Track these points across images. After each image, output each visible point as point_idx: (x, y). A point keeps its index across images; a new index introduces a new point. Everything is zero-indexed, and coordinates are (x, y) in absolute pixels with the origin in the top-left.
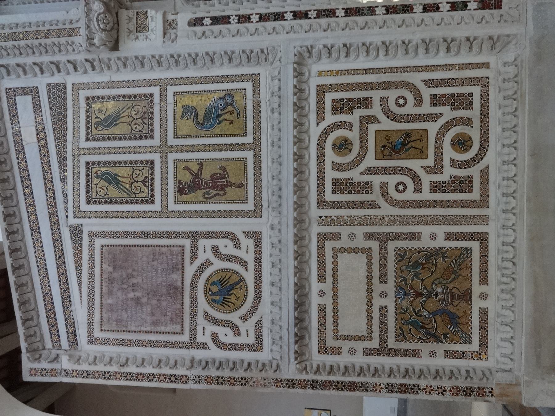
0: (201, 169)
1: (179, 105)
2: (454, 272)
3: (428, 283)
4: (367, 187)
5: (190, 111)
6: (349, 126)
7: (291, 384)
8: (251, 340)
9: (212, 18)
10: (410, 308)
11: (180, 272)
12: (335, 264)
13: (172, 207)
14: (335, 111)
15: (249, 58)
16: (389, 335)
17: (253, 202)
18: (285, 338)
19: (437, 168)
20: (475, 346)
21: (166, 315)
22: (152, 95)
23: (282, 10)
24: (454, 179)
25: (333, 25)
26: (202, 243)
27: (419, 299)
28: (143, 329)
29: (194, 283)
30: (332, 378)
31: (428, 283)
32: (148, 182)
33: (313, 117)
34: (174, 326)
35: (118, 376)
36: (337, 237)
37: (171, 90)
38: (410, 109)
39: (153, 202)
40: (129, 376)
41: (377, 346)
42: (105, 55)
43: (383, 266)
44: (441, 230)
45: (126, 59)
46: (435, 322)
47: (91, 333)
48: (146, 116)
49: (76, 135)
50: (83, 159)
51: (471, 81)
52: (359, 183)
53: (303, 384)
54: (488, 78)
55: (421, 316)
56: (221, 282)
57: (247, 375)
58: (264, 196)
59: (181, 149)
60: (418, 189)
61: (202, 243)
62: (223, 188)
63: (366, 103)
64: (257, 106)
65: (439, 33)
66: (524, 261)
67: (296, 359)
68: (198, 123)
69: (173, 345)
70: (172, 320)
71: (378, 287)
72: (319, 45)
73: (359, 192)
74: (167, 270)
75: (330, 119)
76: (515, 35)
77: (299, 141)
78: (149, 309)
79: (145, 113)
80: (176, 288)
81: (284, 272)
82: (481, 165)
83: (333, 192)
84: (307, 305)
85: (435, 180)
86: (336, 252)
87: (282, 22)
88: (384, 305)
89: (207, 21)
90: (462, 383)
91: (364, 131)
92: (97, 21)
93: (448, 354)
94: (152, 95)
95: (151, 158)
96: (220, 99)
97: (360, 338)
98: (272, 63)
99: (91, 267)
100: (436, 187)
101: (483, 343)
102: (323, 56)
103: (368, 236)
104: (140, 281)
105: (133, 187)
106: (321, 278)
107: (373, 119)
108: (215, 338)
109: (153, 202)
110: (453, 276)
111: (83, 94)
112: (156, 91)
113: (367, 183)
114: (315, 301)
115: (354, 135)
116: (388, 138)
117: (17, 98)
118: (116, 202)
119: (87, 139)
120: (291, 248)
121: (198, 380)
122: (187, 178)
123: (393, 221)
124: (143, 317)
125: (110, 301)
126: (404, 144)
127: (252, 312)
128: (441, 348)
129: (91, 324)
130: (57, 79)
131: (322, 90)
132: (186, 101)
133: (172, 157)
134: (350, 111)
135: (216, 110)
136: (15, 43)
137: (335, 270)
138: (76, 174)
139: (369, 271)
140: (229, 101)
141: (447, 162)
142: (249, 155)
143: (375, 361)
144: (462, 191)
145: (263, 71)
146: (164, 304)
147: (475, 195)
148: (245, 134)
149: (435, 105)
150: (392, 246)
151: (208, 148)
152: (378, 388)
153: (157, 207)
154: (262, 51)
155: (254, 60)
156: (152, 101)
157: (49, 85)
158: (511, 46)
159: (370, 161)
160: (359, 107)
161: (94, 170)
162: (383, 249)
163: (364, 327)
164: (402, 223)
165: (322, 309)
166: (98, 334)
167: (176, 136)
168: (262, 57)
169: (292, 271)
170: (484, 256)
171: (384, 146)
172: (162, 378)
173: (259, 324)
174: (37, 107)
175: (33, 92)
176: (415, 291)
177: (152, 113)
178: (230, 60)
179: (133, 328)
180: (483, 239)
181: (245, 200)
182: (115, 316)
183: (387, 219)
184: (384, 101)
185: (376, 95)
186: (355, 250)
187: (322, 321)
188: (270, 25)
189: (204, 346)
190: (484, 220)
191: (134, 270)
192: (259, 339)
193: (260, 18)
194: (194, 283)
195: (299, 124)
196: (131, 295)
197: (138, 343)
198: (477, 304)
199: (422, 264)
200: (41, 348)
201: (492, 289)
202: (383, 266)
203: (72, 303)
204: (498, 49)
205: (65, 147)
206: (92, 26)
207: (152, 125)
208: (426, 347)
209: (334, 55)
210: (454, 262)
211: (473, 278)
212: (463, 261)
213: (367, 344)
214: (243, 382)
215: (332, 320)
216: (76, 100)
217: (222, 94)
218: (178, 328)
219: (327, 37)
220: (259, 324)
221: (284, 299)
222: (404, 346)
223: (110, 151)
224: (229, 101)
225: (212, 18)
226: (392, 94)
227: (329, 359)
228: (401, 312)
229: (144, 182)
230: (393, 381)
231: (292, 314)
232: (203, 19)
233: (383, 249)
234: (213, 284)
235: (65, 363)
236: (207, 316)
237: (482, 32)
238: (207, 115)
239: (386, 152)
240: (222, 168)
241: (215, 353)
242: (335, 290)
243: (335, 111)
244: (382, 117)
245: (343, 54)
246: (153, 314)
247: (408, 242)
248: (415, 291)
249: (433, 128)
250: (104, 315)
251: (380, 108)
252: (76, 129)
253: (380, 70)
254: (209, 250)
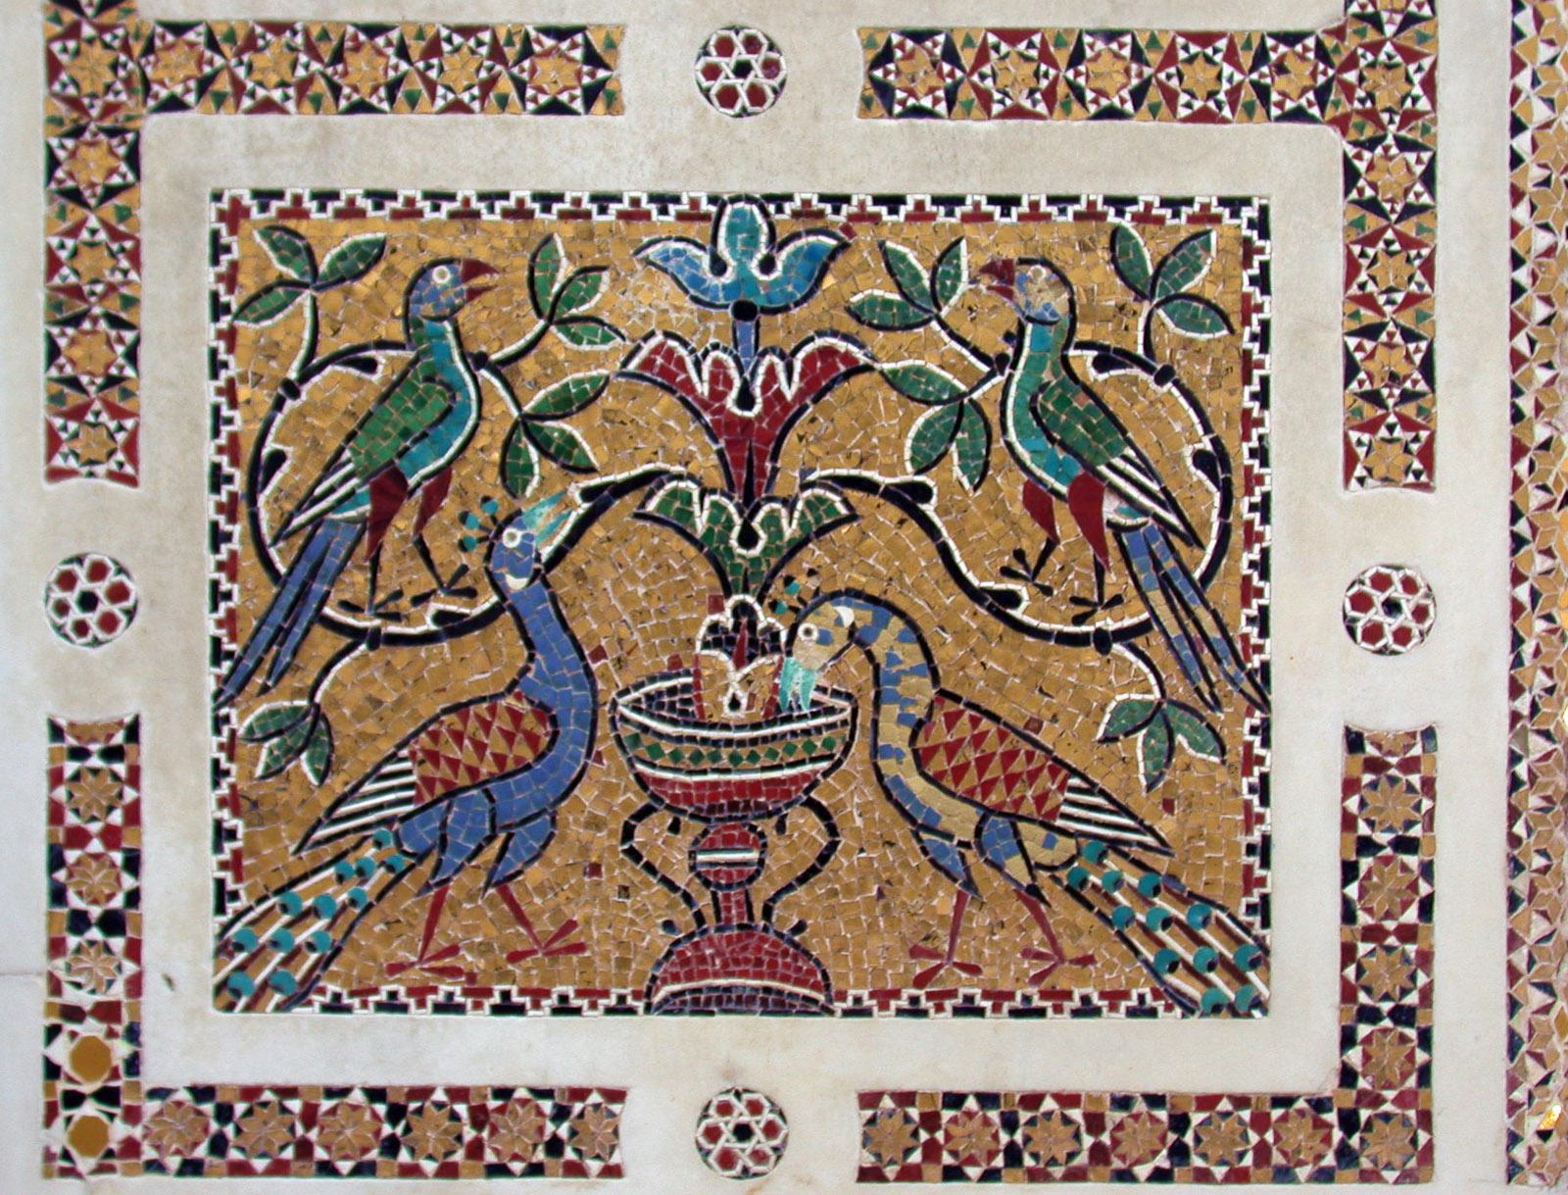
10: (601, 359)
16: (294, 126)
27: (706, 459)
46: (452, 626)
55: (512, 474)
88: (628, 75)
199: (1087, 495)
210: (1104, 823)
211: (942, 1024)
212: (1116, 924)
247: (1332, 342)
248: (783, 417)
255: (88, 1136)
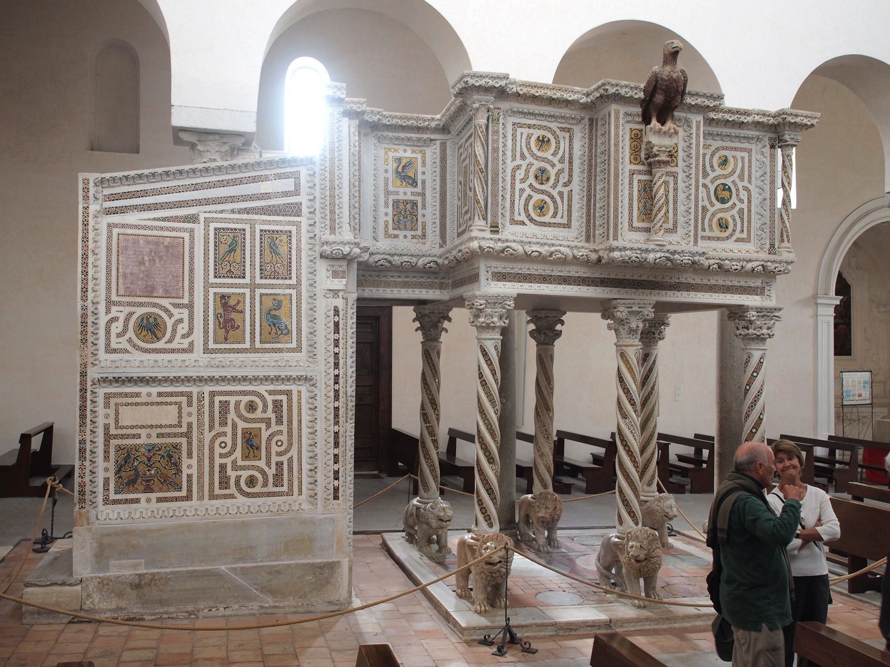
0: (239, 312)
1: (282, 298)
2: (165, 481)
3: (158, 464)
4: (223, 423)
5: (279, 306)
6: (264, 411)
7: (83, 375)
8: (113, 345)
9: (338, 322)
11: (164, 295)
12: (171, 404)
13: (212, 291)
14: (275, 402)
15: (311, 346)
17: (214, 348)
18: (117, 370)
19: (235, 467)
20: (113, 496)
21: (132, 284)
22: (290, 278)
23: (340, 367)
24: (228, 478)
25: (329, 400)
26: (186, 312)
27: (146, 459)
28: (120, 266)
29: (155, 305)
30: (89, 402)
31: (158, 464)
32: (230, 274)
33: (271, 387)
34: (123, 290)
35: (85, 248)
36: (190, 404)
37: (293, 292)
38: (274, 449)
39: (215, 277)
40: (85, 257)
41: (111, 433)
42: (318, 248)
43: (169, 435)
44: (194, 471)
45: (315, 263)
46: (130, 470)
47: (116, 225)
48: (277, 274)
49: (265, 222)
50: (247, 227)
51: (291, 485)
52: (226, 418)
53: (83, 383)
54: (292, 495)
55: (134, 461)
56: (157, 325)
57: (89, 344)
58: (219, 355)
59: (253, 298)
60: (222, 456)
61: (186, 312)
62: (224, 327)
63: (279, 421)
64: (280, 350)
65: (320, 464)
66: (174, 522)
67: (102, 378)
68: (270, 311)
69: (109, 288)
70: (127, 288)
71: (154, 432)
72: (316, 391)
73: (220, 418)
74: (165, 286)
75: (270, 399)
76: (317, 508)
77: (256, 379)
78: (136, 271)
79: (278, 273)
80: (152, 292)
81: (165, 369)
82: (237, 494)
83: (220, 402)
84: (141, 385)
85: (228, 466)
86: (179, 404)
87: (333, 368)
88: (141, 436)
89: (336, 319)
90: (88, 488)
91: (261, 420)
92: (338, 249)
93: (107, 480)
94: (290, 278)
95: (246, 277)
96: (286, 326)
97: (117, 421)
98: (307, 361)
99: (167, 229)
100: (223, 467)
101: (115, 502)
102: (311, 393)
103: (190, 425)
104: (157, 265)
105: (226, 263)
106: (160, 394)
107: (269, 426)
108: (114, 319)
109: (215, 277)
110: (163, 480)
111: (293, 229)
112: (294, 281)
113: (226, 423)
114: (144, 390)
115: (258, 414)
116: (256, 436)
117: (293, 180)
118: (215, 250)
119: (261, 231)
120: (182, 374)
121: (84, 308)
122: (232, 302)
123: (200, 441)
124: (130, 266)
125: (141, 242)
126: (252, 446)
127: (135, 346)
128: (111, 475)
129: (123, 226)
130: (305, 210)
131: (288, 393)
132: (285, 303)
133: (247, 292)
134: (274, 411)
135: (278, 323)
136: (328, 188)
137: (166, 404)
138: (238, 221)
139: (166, 426)
140: (284, 332)
141: (239, 473)
142: (247, 345)
143: (100, 431)
144: (220, 483)
145: (303, 355)
146: (140, 283)
147: (217, 491)
148: (261, 342)
149: (277, 464)
150: (184, 440)
151: (253, 316)
152: (82, 434)
153: (212, 280)
154: (315, 355)
155: (310, 349)
156: (286, 278)
157: (301, 204)
158: (311, 507)
159: (241, 425)
160: (276, 417)
161: (239, 235)
162: (182, 435)
163: (125, 424)
164: (199, 446)
165: (138, 395)
166: (115, 231)
167: (262, 295)
168: (311, 355)
169: (166, 375)
170: (176, 499)
171: (250, 433)
172: (85, 281)
173: (127, 351)
174: (286, 194)
175: (297, 192)
176: (151, 457)
177: (278, 278)
178: (311, 333)
179: (120, 259)
180: (188, 498)
181: (215, 342)
182: (130, 245)
183: (202, 436)
184: (280, 432)
185: (284, 428)
186: (180, 417)
187: (129, 396)
188: (332, 360)
189: (108, 311)
190: (201, 498)
191: (165, 261)
192: (115, 351)
193: (336, 354)
194: (155, 305)
195: (266, 379)
196: (146, 258)
197: (109, 261)
198: (143, 496)
199: (171, 460)
200: (103, 186)
201: (154, 505)
202: (169, 435)
203: (140, 212)
204: (309, 500)
205: (257, 213)
206: (335, 245)
207: (270, 278)
208: (111, 465)
209: (311, 400)
210: (172, 480)
213: (112, 426)
214: (84, 341)
215: (130, 402)
216: (289, 223)
217: (289, 327)
218: (121, 292)
219: (321, 396)
220: (127, 351)
221: (146, 370)
222: (112, 451)
223: (253, 246)
224: (284, 332)
225: (338, 322)
226: (284, 438)
227: (101, 400)
228: (136, 448)
229: (230, 271)
230: (88, 443)
231: (135, 375)
232: (338, 316)
233: (182, 435)
234: (155, 319)
235: (94, 208)
236: (131, 314)
237: (320, 489)
238: (275, 317)
239: (247, 435)
240: (239, 326)
241: (103, 319)
242: (152, 404)
243: (275, 402)
244: (270, 431)
245: (311, 406)
246: (132, 274)
247: (186, 450)
248: (151, 457)
249: (262, 464)
250: (131, 237)
251: (275, 430)
252: (269, 223)
253: (300, 429)
254: (181, 316)
255: (106, 503)
